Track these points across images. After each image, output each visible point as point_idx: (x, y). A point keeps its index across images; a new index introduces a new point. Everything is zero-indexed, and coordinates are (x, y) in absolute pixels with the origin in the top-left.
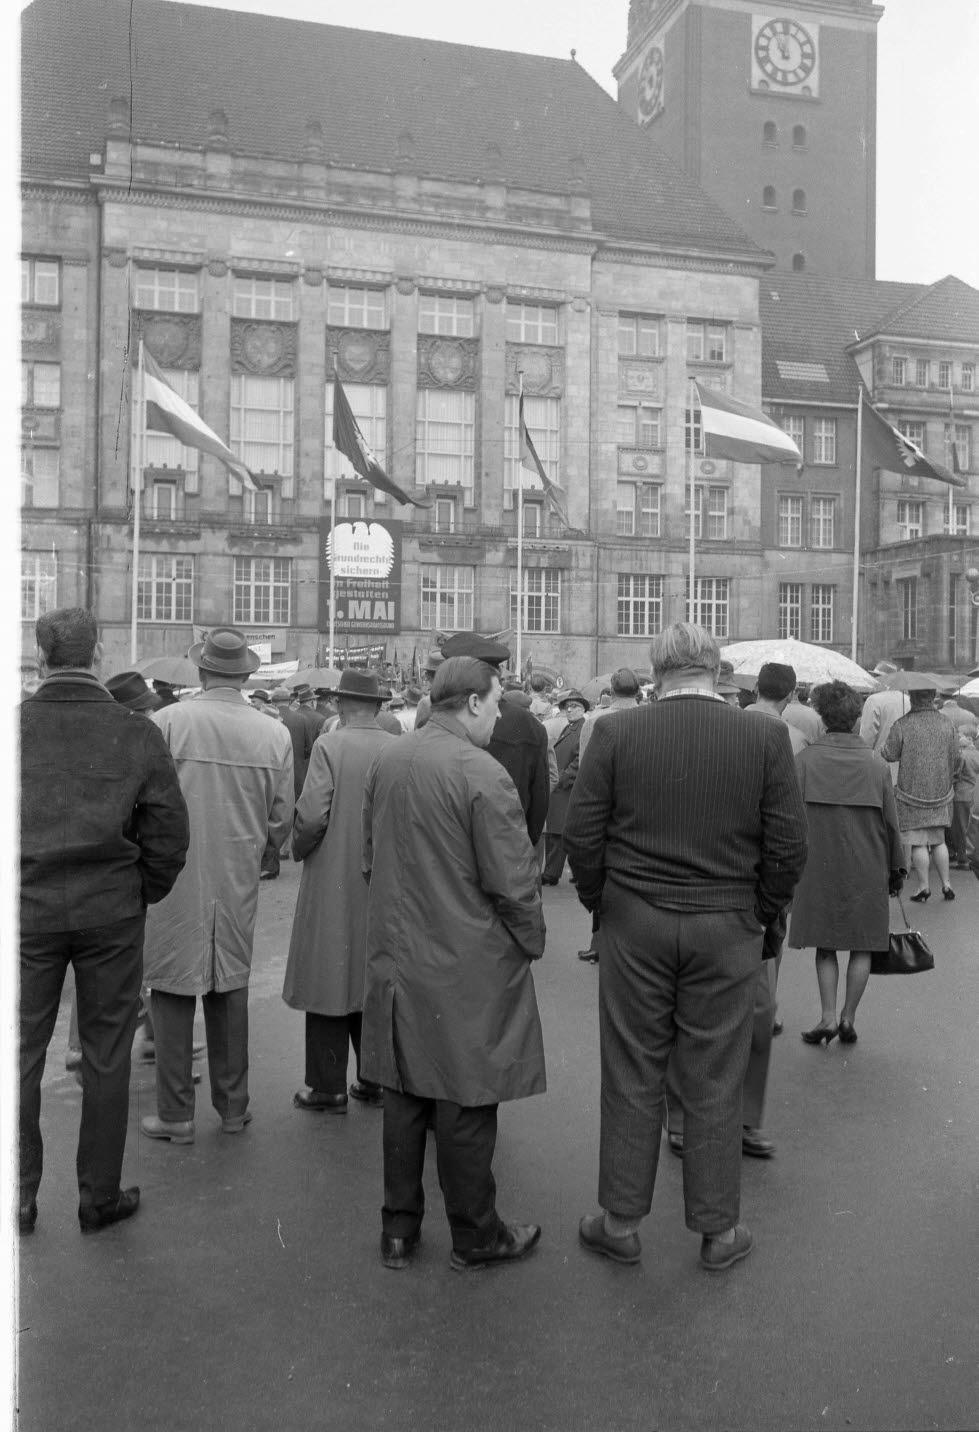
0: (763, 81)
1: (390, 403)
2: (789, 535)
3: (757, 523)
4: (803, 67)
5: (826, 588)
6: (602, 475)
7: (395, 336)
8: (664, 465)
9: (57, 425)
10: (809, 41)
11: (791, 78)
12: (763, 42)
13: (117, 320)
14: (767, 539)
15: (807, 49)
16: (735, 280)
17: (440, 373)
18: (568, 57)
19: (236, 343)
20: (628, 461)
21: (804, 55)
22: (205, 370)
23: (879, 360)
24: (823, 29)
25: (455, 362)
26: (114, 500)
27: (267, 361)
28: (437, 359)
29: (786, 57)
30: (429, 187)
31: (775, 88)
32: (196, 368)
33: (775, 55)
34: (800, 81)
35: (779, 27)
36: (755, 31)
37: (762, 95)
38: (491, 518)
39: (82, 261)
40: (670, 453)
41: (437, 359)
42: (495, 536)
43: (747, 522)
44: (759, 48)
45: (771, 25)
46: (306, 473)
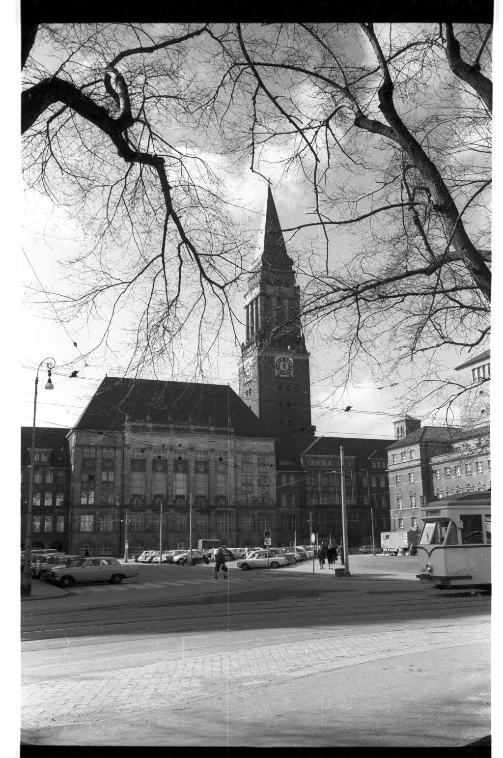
0: (278, 374)
1: (188, 476)
2: (284, 502)
3: (276, 502)
4: (289, 369)
5: (294, 517)
6: (238, 492)
7: (190, 462)
8: (252, 489)
9: (114, 485)
10: (290, 363)
11: (286, 373)
12: (278, 364)
13: (128, 462)
14: (278, 504)
15: (290, 365)
16: (269, 444)
17: (200, 470)
18: (227, 385)
19: (154, 465)
20: (244, 488)
21: (289, 367)
22: (147, 472)
23: (305, 460)
24: (294, 360)
25: (203, 467)
26: (127, 502)
27: (160, 469)
28: (199, 467)
29: (285, 368)
30: (197, 427)
31: (282, 376)
32: (145, 471)
33: (281, 367)
34: (288, 373)
35: (282, 360)
36: (276, 361)
37: (278, 377)
38: (212, 503)
39: (120, 448)
40: (254, 486)
41: (199, 467)
42: (213, 508)
43: (273, 502)
44: (277, 365)
45: (280, 359)
46: (170, 493)
